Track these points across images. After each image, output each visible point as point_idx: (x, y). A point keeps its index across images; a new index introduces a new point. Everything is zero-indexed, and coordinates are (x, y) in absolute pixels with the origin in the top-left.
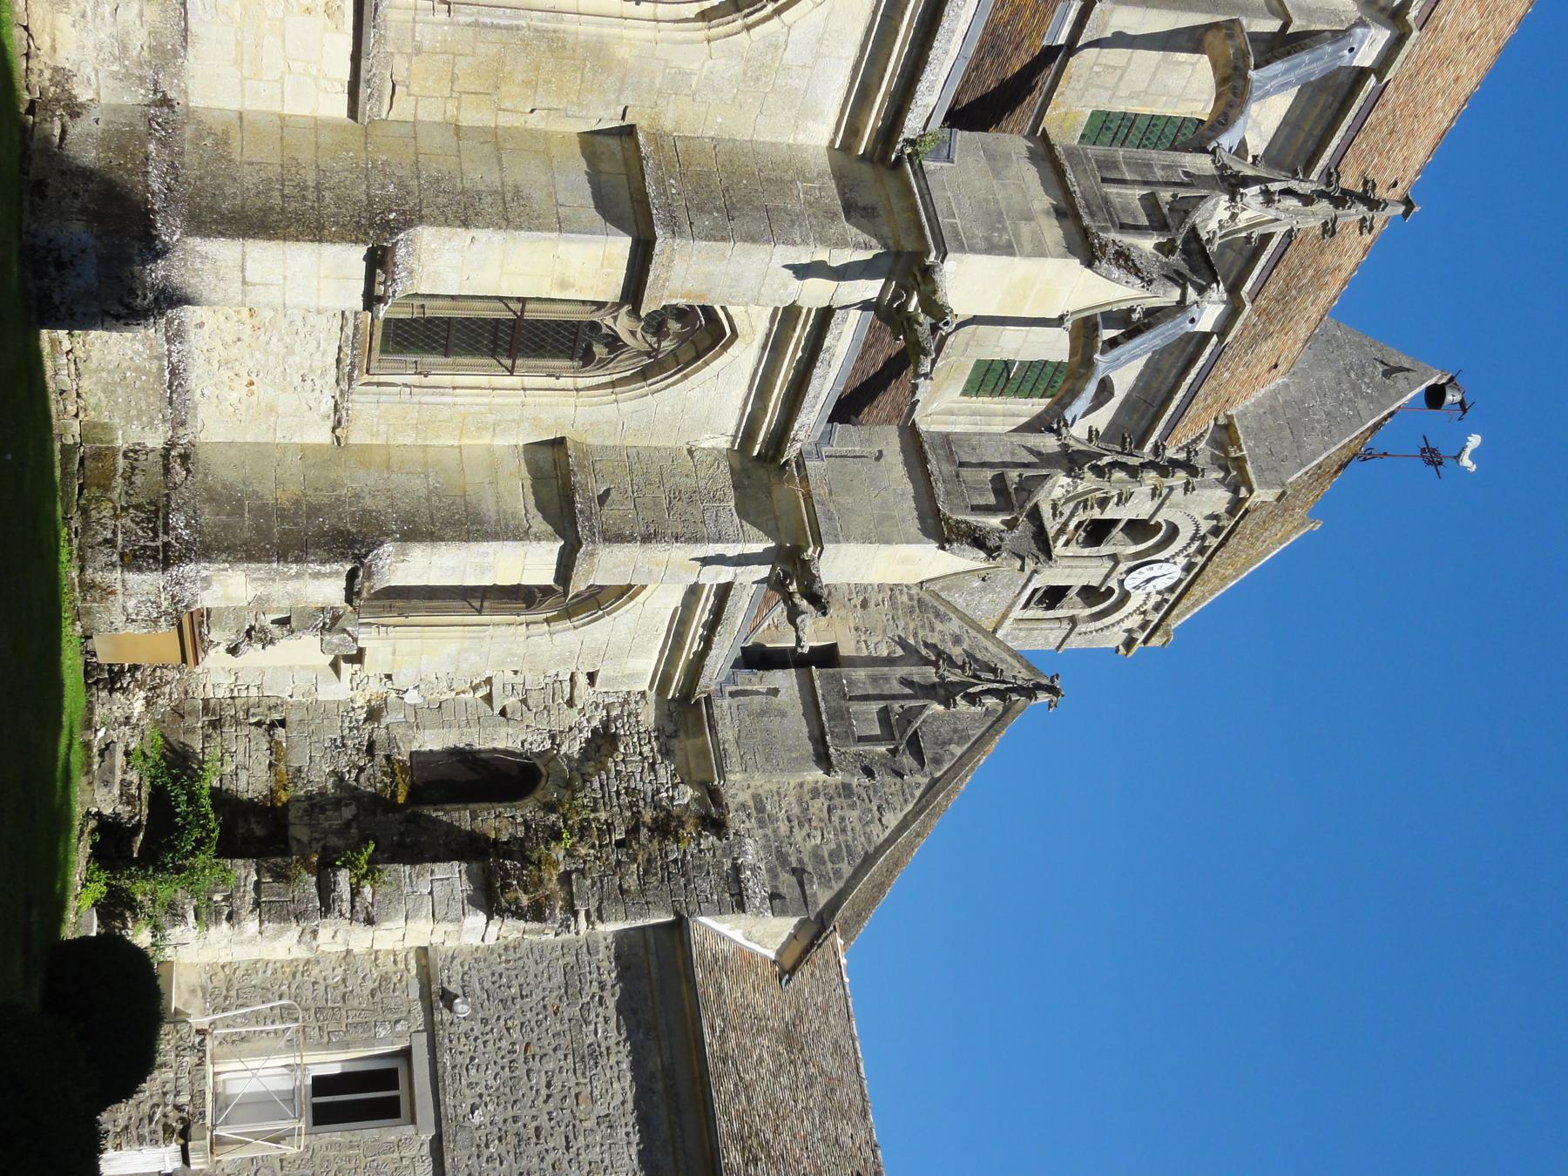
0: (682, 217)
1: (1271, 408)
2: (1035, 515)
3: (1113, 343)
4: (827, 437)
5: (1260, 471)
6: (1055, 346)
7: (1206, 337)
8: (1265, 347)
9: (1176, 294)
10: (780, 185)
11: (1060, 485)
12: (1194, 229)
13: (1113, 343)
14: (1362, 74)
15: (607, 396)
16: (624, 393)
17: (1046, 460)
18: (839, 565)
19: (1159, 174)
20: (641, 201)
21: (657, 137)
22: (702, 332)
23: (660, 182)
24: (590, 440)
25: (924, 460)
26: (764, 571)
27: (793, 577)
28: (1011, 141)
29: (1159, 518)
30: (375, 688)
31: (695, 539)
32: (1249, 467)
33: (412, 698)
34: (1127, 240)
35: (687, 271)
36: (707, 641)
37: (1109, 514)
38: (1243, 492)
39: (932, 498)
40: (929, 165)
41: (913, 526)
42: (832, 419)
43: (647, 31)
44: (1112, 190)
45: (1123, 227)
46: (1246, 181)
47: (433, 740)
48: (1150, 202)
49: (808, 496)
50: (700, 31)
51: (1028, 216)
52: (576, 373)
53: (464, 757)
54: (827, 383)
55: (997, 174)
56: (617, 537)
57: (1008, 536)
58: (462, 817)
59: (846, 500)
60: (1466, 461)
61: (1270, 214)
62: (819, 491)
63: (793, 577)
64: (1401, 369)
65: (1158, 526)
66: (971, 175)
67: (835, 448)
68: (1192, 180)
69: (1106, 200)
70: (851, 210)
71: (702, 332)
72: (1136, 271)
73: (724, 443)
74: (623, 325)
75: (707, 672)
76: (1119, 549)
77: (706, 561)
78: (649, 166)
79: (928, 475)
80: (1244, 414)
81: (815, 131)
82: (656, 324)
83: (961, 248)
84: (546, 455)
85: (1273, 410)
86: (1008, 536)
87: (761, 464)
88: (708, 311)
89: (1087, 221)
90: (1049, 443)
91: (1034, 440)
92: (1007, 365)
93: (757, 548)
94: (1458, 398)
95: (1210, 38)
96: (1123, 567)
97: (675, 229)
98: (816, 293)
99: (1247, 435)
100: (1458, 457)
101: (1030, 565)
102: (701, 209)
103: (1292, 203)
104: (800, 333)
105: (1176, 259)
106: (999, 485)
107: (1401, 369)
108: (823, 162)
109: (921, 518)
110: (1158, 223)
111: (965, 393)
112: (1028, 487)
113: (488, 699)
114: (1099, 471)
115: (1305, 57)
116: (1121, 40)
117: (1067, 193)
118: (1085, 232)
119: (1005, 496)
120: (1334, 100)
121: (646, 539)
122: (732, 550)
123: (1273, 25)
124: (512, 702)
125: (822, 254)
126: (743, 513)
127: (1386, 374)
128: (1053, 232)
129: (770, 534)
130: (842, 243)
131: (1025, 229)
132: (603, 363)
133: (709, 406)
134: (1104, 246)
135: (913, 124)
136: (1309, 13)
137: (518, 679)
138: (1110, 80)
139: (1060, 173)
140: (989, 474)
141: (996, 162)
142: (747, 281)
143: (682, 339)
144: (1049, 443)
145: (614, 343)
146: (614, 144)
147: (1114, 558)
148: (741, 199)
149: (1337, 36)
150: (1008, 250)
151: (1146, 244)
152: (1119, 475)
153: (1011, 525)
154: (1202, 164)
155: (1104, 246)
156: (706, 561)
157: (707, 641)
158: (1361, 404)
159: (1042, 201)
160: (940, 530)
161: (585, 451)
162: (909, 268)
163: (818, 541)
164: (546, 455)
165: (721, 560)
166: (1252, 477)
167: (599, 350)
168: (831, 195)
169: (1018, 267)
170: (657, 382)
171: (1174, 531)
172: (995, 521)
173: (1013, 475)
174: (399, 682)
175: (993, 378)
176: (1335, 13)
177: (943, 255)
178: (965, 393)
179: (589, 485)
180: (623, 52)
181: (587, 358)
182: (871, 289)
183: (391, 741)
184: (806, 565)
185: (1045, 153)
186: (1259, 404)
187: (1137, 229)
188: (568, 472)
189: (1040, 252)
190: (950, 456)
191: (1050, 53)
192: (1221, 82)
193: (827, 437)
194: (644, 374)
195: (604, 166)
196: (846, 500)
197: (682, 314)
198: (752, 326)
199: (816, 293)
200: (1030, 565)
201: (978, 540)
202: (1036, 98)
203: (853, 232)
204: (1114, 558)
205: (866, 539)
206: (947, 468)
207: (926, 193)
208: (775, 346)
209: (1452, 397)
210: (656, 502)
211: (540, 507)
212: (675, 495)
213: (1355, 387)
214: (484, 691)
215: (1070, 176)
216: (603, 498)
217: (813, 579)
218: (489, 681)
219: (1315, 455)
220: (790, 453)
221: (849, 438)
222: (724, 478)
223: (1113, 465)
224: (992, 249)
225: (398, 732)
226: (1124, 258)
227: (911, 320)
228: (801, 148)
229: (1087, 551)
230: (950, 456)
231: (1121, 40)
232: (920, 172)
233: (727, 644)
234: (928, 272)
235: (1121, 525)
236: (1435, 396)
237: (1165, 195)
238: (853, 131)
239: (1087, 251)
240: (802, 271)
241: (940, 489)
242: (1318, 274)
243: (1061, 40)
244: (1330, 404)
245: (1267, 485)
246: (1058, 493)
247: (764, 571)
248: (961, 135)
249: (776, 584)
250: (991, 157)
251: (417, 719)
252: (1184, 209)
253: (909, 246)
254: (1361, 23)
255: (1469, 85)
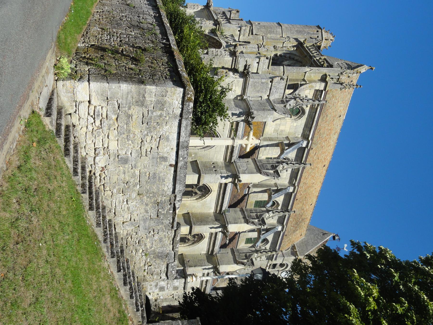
0: (195, 223)
1: (302, 242)
2: (252, 260)
3: (264, 234)
4: (220, 251)
5: (300, 253)
6: (255, 235)
7: (280, 232)
8: (298, 232)
9: (260, 227)
10: (208, 218)
11: (256, 255)
12: (263, 218)
13: (264, 234)
14: (292, 193)
15: (188, 247)
16: (190, 246)
17: (253, 252)
18: (223, 268)
19: (258, 211)
20: (190, 221)
21: (192, 213)
22: (200, 237)
23: (193, 219)
24: (187, 254)
25: (234, 253)
26: (212, 270)
27: (216, 271)
28: (238, 209)
29: (284, 262)
30: (156, 296)
31: (202, 266)
32: (298, 252)
33: (161, 298)
34: (254, 220)
35: (197, 230)
36: (206, 284)
37: (274, 262)
38: (297, 257)
39: (236, 258)
40: (226, 213)
41: (233, 262)
42: (220, 248)
43: (190, 202)
44: (251, 214)
45: (253, 219)
46: (270, 211)
47: (165, 304)
48: (257, 215)
49: (217, 259)
50: (196, 201)
51: (240, 219)
52: (184, 244)
53: (169, 306)
54: (218, 243)
55: (236, 213)
56: (190, 266)
57: (248, 263)
58: (171, 315)
59: (223, 259)
60: (345, 249)
61: (274, 215)
62: (219, 258)
63: (216, 271)
64: (326, 234)
65: (284, 265)
66: (232, 214)
67: (221, 252)
68: (263, 211)
69: (251, 215)
70: (216, 220)
71: (200, 237)
72: (255, 224)
73: (205, 252)
74: (189, 237)
75: (207, 290)
76: (279, 269)
77: (203, 269)
78: (191, 217)
79: (235, 255)
80: (297, 244)
81: (212, 210)
82: (194, 236)
83: (231, 224)
84: (180, 256)
85: (302, 243)
86: (248, 263)
87: (210, 256)
88: (201, 234)
89: (247, 218)
90: (253, 249)
91: (251, 249)
92: (251, 239)
93: (211, 267)
94: (338, 238)
95: (267, 191)
96: (280, 272)
97: (195, 224)
98: (213, 231)
99: (298, 247)
100: (343, 249)
101: (251, 267)
102: (198, 222)
103: (277, 213)
104: (213, 236)
105: (260, 222)
106: (246, 256)
107: (326, 234)
108: (212, 214)
109: (234, 261)
110: (258, 218)
111: (245, 244)
112: (250, 256)
113: (173, 297)
114: (261, 253)
115: (280, 192)
116: (255, 192)
117: (245, 215)
118: (247, 220)
119: (247, 257)
120: (288, 196)
121: (195, 266)
122: (207, 267)
123: (276, 188)
124: (177, 297)
125: (213, 226)
126: (208, 262)
127: (323, 235)
128: (243, 220)
129: (212, 265)
130: (216, 224)
131: (239, 220)
132: (187, 243)
133: (202, 247)
134: (250, 222)
135: (223, 209)
136: (280, 186)
137: (177, 294)
138: (256, 197)
139: (244, 212)
140: (244, 254)
141: (235, 212)
142: (205, 230)
143: (198, 238)
144: (253, 249)
145: (189, 240)
146: (187, 215)
147: (278, 271)
148: (203, 220)
149: (285, 189)
150: (237, 223)
151: (256, 220)
152: (264, 253)
153: (248, 261)
154: (264, 209)
155: (250, 222)
156: (203, 269)
157: (206, 284)
158: (318, 240)
159: (241, 216)
160: (236, 262)
161: (186, 255)
162: (224, 227)
163: (219, 265)
164: (180, 256)
165: (206, 269)
166: (298, 254)
167: (187, 241)
168: (214, 219)
169: (239, 225)
170: (195, 244)
171: (287, 265)
172: (246, 261)
173: (248, 254)
174: (159, 295)
175: (249, 241)
176: (285, 185)
177: (228, 225)
178: (245, 244)
179: (186, 260)
180: (187, 204)
181: (185, 242)
182: (220, 229)
183: (159, 304)
184: (217, 268)
185: (242, 211)
186: (300, 242)
187: (255, 219)
188: (183, 258)
189: (241, 223)
190: (238, 252)
191: (245, 195)
192: (269, 197)
193: (220, 251)
194: (193, 244)
195: (186, 218)
196: (223, 259)
197: (198, 235)
198: (207, 236)
199: (213, 231)
200: (251, 267)
201: (243, 264)
202: (245, 200)
203: (217, 223)
204: (278, 271)
205: (226, 264)
206: (238, 254)
207: (226, 217)
208: (210, 238)
209: (336, 238)
210: (196, 261)
211: (180, 263)
212: (199, 260)
213: (317, 237)
214: (172, 296)
215: (245, 213)
216: (188, 261)
217: (219, 270)
218: (173, 294)
219: (310, 250)
220: (214, 253)
221: (223, 250)
222: (205, 258)
223: (264, 252)
224: (235, 223)
225: (160, 303)
226: (253, 223)
227: (225, 233)
228: (210, 213)
229: (273, 270)
230: (238, 252)
231: (255, 192)
232: (225, 215)
233: (209, 285)
234: (226, 227)
235: (279, 265)
236: (334, 238)
237: (259, 214)
238: (216, 210)
239: (247, 222)
240: (211, 228)
241: (237, 257)
242: (303, 220)
243: (247, 193)
244: (313, 241)
245: (302, 255)
246: (256, 256)
247: (212, 270)
248: (231, 209)
249: (214, 272)
250: (235, 211)
251: (163, 301)
252: (261, 215)
253: (224, 224)
254: (289, 186)
255: (319, 189)
